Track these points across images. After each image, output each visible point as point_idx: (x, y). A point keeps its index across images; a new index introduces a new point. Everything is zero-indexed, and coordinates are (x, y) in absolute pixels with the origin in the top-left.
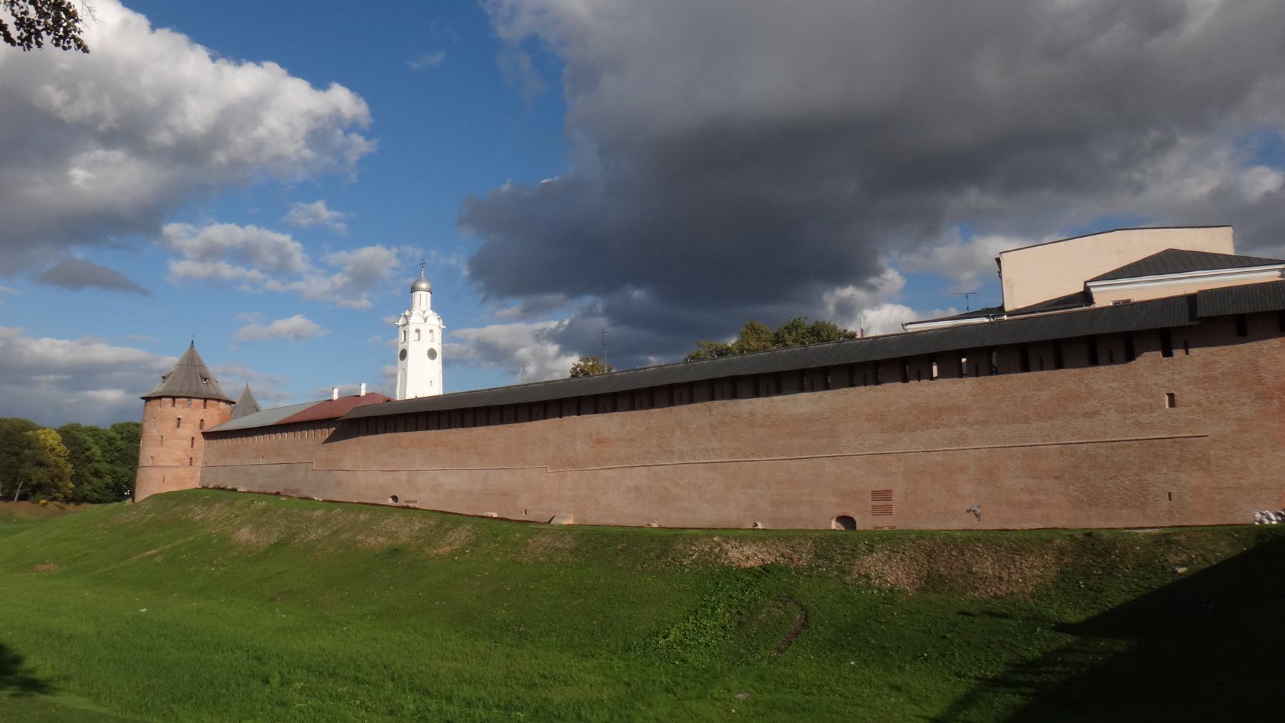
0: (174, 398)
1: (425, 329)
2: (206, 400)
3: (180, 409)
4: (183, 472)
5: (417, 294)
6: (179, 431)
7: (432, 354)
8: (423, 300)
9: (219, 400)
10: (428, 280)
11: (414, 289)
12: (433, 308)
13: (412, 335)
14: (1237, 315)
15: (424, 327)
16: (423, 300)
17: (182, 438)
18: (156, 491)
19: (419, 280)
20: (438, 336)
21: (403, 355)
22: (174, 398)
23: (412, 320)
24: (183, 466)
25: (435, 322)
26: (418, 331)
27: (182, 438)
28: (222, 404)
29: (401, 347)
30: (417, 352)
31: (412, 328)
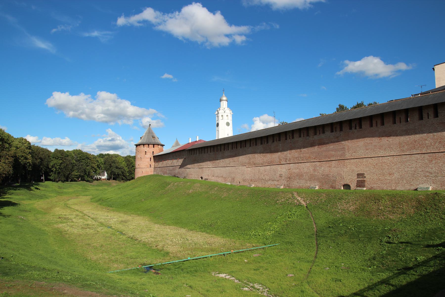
0: (149, 145)
1: (225, 115)
2: (154, 145)
3: (146, 148)
4: (148, 170)
5: (222, 102)
6: (146, 156)
7: (228, 124)
8: (224, 104)
9: (158, 145)
10: (226, 96)
11: (221, 100)
12: (228, 107)
13: (220, 117)
14: (419, 107)
15: (225, 113)
16: (224, 104)
17: (147, 158)
18: (140, 176)
19: (222, 96)
20: (230, 118)
21: (218, 125)
22: (144, 145)
23: (220, 112)
24: (148, 167)
25: (229, 112)
26: (222, 116)
27: (147, 158)
28: (160, 146)
29: (217, 122)
30: (222, 124)
31: (220, 115)
